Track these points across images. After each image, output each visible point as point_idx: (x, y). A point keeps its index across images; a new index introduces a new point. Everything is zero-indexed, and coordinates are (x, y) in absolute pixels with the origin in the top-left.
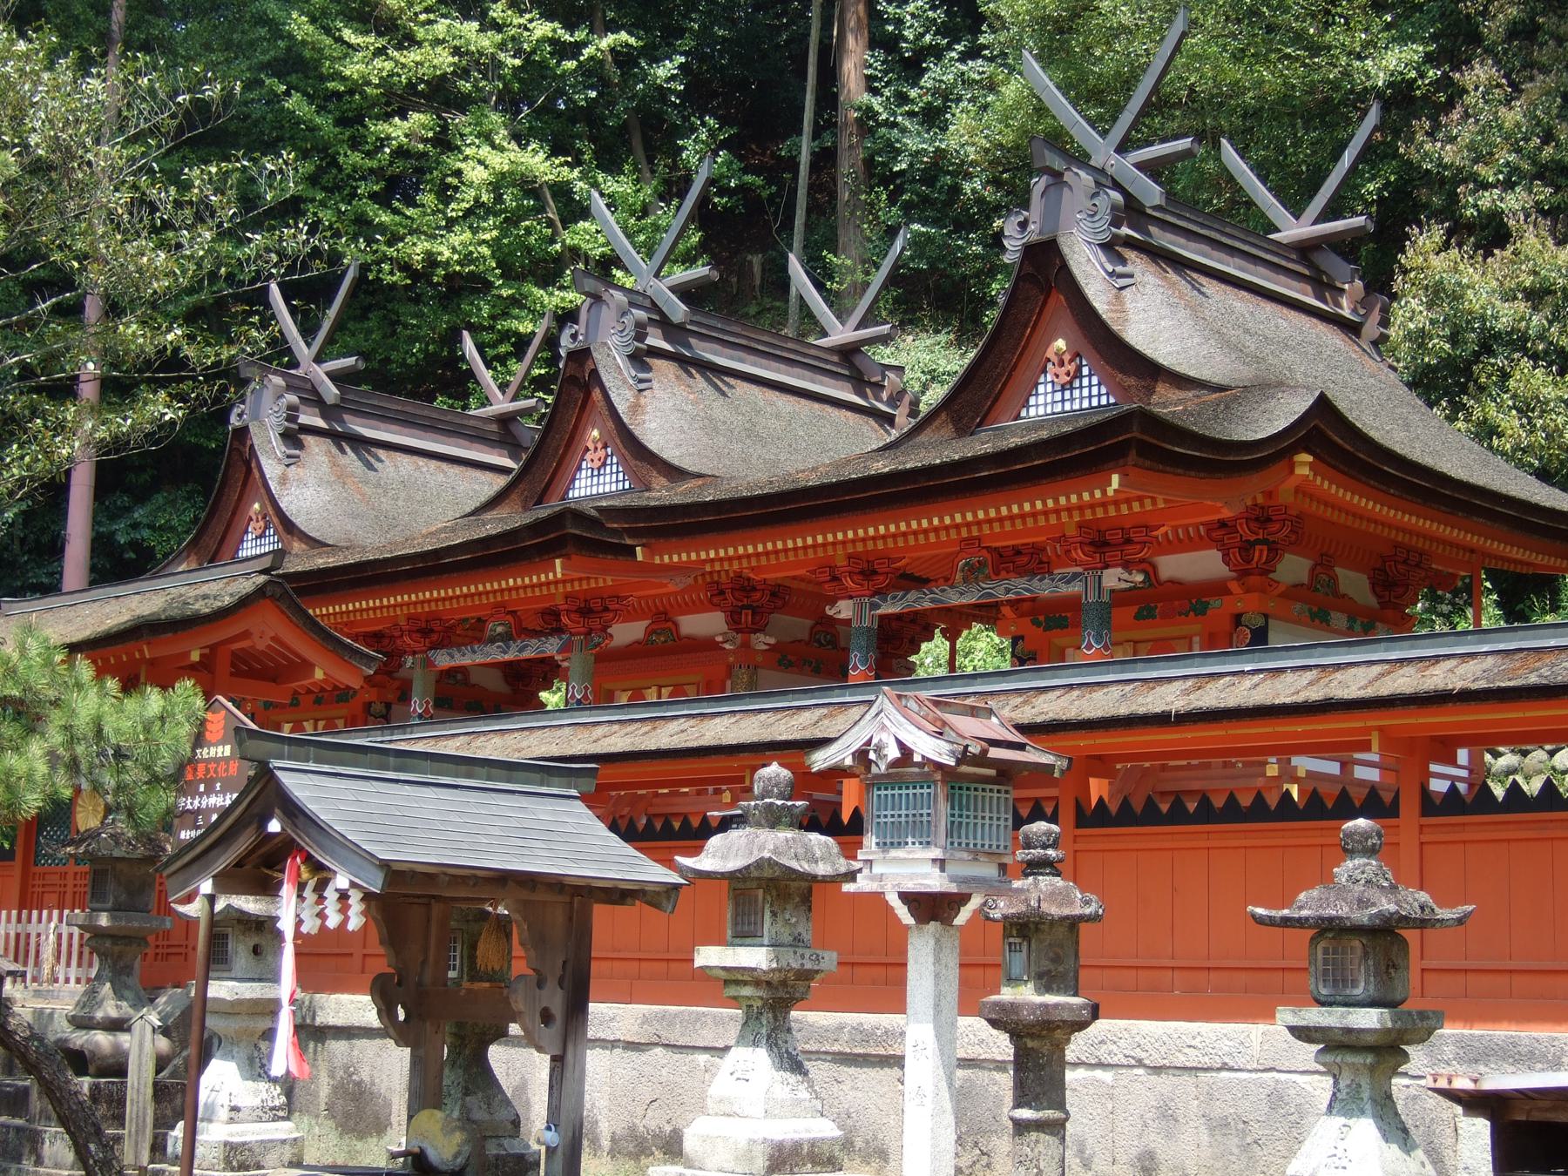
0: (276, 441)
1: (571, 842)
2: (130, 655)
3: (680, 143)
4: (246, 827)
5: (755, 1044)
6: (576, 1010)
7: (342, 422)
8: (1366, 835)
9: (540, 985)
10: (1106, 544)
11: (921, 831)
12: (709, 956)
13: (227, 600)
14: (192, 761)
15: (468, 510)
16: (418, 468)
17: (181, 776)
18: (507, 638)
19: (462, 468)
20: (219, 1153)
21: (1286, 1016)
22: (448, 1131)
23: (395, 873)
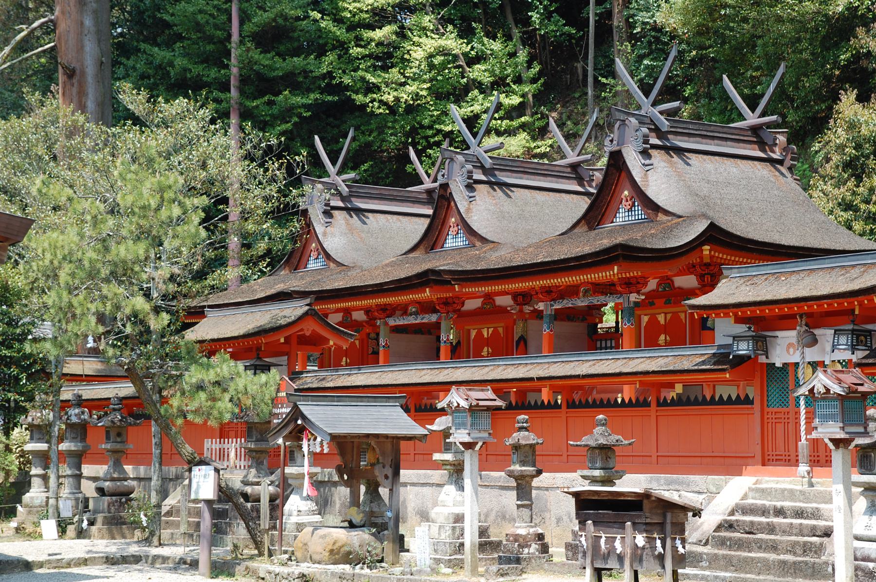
0: (321, 216)
1: (392, 420)
2: (258, 341)
3: (530, 14)
5: (451, 484)
6: (396, 474)
7: (350, 202)
8: (601, 420)
9: (384, 467)
10: (631, 284)
12: (437, 456)
13: (293, 318)
14: (277, 397)
15: (404, 252)
16: (388, 220)
17: (275, 401)
18: (416, 314)
19: (410, 218)
20: (294, 527)
21: (580, 472)
22: (358, 514)
23: (334, 438)
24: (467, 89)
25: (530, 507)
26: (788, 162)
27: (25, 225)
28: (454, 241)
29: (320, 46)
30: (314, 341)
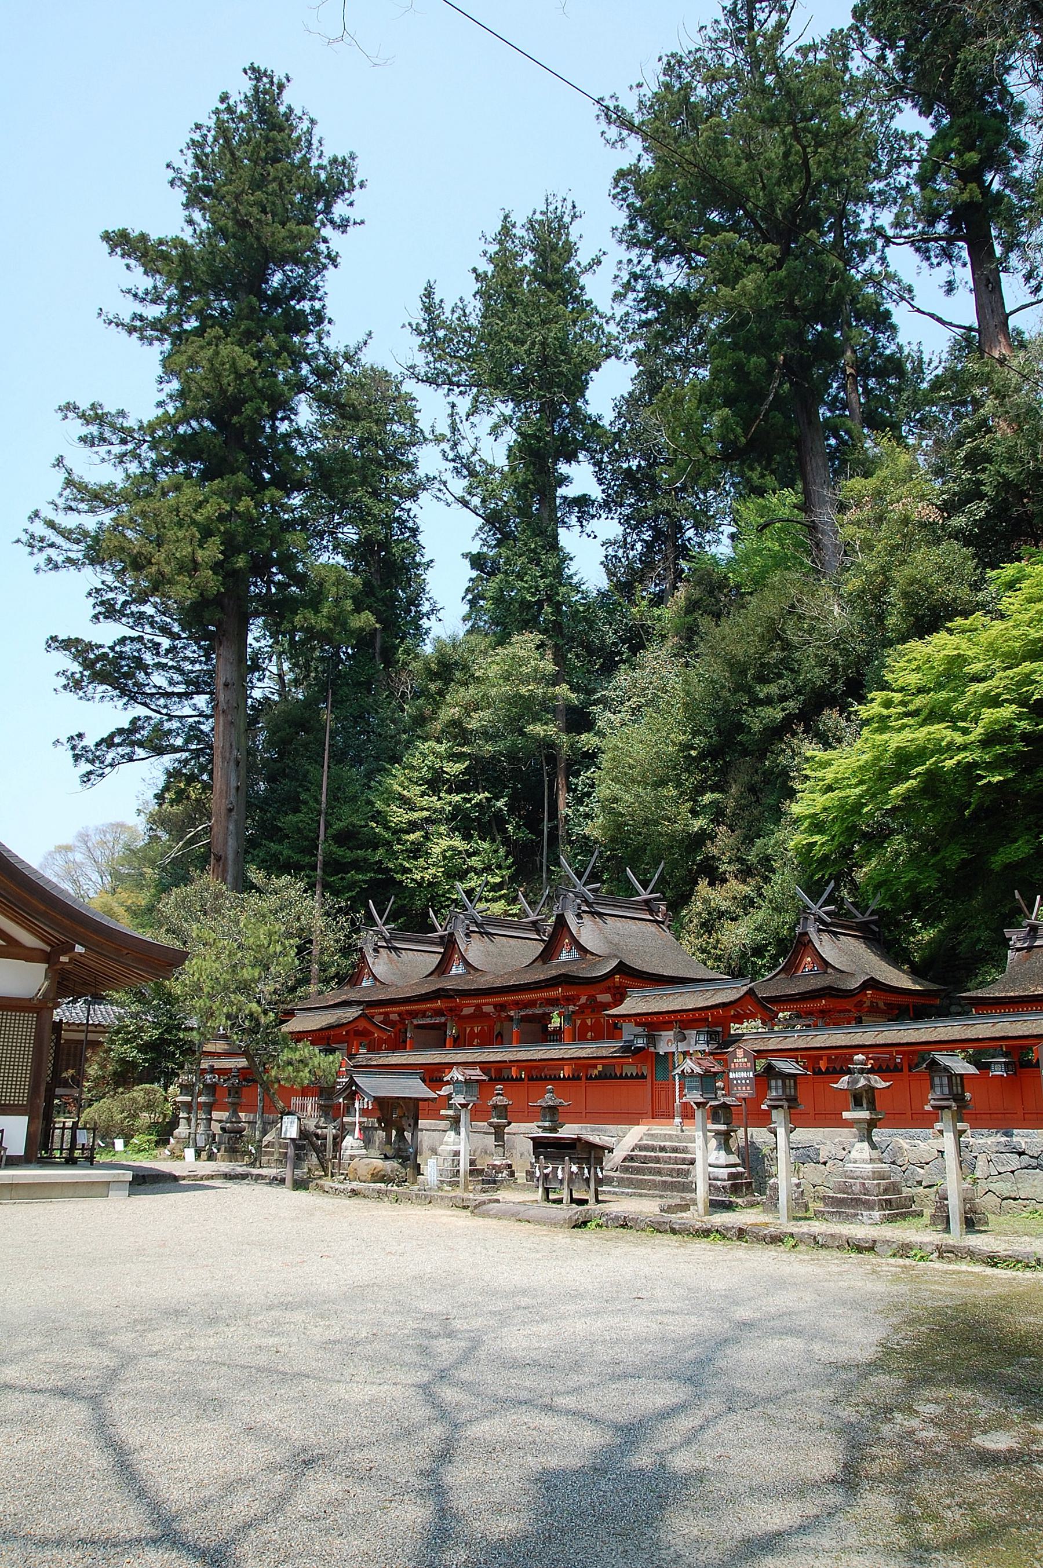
1: (415, 1088)
6: (417, 1123)
12: (443, 1112)
17: (338, 1074)
24: (467, 872)
25: (503, 1146)
26: (667, 923)
27: (183, 956)
28: (457, 970)
29: (374, 843)
30: (364, 1034)
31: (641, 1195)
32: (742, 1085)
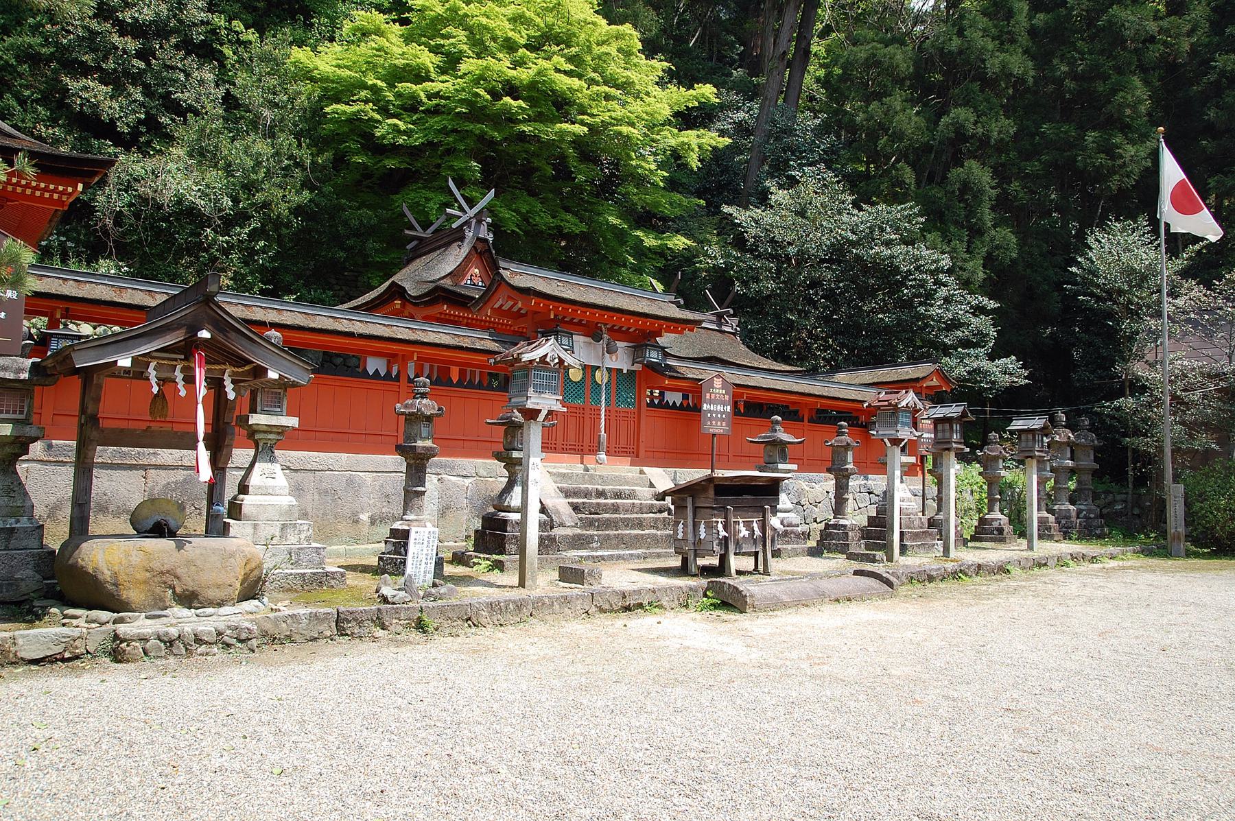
4: (178, 329)
11: (553, 390)
31: (619, 557)
32: (716, 419)
